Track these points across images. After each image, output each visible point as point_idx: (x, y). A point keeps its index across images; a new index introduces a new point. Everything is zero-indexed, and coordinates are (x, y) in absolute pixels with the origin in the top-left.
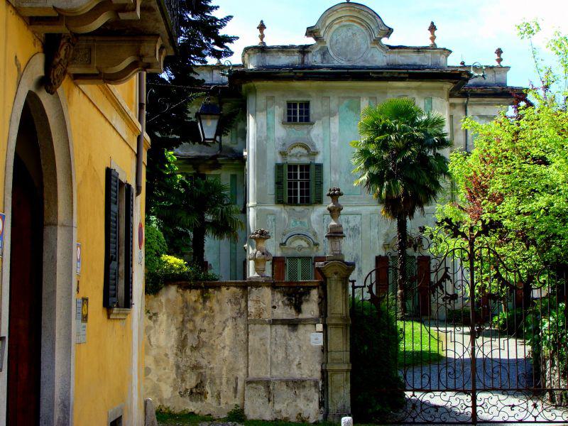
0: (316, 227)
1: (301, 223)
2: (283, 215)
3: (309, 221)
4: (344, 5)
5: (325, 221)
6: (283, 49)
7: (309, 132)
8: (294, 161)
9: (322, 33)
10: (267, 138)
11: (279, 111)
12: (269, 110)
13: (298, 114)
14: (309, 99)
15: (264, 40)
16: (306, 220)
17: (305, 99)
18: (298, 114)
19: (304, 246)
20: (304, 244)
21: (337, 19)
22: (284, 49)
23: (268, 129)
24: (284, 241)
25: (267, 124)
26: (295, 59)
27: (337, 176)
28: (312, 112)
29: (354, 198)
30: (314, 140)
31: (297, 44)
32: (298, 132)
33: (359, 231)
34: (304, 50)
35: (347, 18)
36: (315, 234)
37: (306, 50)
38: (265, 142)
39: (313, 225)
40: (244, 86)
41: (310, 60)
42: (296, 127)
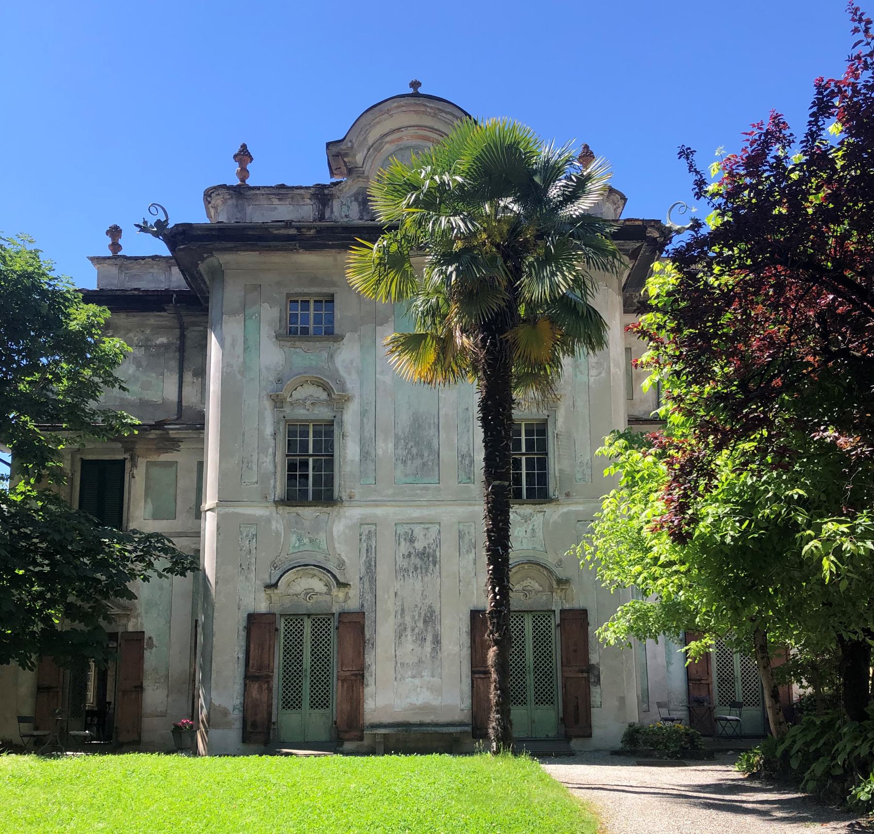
0: (343, 550)
1: (311, 541)
2: (274, 525)
3: (330, 538)
4: (403, 101)
5: (364, 538)
6: (282, 191)
7: (331, 357)
8: (301, 413)
9: (359, 158)
10: (245, 369)
11: (270, 314)
12: (249, 311)
13: (312, 320)
14: (332, 290)
15: (247, 182)
16: (322, 537)
17: (325, 290)
18: (312, 320)
19: (317, 590)
20: (318, 585)
21: (393, 131)
22: (282, 191)
23: (246, 349)
24: (273, 581)
25: (246, 340)
26: (307, 211)
27: (391, 445)
28: (338, 314)
29: (426, 489)
30: (342, 372)
31: (311, 184)
32: (308, 356)
33: (434, 557)
34: (322, 195)
35: (411, 131)
36: (341, 564)
37: (326, 192)
38: (239, 377)
39: (337, 545)
40: (202, 267)
41: (336, 212)
42: (305, 345)
